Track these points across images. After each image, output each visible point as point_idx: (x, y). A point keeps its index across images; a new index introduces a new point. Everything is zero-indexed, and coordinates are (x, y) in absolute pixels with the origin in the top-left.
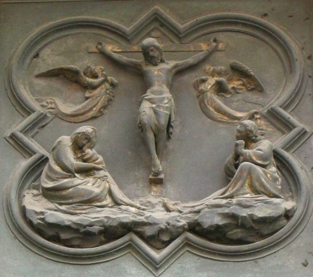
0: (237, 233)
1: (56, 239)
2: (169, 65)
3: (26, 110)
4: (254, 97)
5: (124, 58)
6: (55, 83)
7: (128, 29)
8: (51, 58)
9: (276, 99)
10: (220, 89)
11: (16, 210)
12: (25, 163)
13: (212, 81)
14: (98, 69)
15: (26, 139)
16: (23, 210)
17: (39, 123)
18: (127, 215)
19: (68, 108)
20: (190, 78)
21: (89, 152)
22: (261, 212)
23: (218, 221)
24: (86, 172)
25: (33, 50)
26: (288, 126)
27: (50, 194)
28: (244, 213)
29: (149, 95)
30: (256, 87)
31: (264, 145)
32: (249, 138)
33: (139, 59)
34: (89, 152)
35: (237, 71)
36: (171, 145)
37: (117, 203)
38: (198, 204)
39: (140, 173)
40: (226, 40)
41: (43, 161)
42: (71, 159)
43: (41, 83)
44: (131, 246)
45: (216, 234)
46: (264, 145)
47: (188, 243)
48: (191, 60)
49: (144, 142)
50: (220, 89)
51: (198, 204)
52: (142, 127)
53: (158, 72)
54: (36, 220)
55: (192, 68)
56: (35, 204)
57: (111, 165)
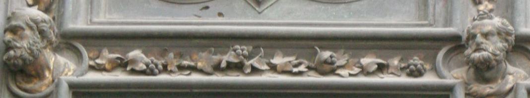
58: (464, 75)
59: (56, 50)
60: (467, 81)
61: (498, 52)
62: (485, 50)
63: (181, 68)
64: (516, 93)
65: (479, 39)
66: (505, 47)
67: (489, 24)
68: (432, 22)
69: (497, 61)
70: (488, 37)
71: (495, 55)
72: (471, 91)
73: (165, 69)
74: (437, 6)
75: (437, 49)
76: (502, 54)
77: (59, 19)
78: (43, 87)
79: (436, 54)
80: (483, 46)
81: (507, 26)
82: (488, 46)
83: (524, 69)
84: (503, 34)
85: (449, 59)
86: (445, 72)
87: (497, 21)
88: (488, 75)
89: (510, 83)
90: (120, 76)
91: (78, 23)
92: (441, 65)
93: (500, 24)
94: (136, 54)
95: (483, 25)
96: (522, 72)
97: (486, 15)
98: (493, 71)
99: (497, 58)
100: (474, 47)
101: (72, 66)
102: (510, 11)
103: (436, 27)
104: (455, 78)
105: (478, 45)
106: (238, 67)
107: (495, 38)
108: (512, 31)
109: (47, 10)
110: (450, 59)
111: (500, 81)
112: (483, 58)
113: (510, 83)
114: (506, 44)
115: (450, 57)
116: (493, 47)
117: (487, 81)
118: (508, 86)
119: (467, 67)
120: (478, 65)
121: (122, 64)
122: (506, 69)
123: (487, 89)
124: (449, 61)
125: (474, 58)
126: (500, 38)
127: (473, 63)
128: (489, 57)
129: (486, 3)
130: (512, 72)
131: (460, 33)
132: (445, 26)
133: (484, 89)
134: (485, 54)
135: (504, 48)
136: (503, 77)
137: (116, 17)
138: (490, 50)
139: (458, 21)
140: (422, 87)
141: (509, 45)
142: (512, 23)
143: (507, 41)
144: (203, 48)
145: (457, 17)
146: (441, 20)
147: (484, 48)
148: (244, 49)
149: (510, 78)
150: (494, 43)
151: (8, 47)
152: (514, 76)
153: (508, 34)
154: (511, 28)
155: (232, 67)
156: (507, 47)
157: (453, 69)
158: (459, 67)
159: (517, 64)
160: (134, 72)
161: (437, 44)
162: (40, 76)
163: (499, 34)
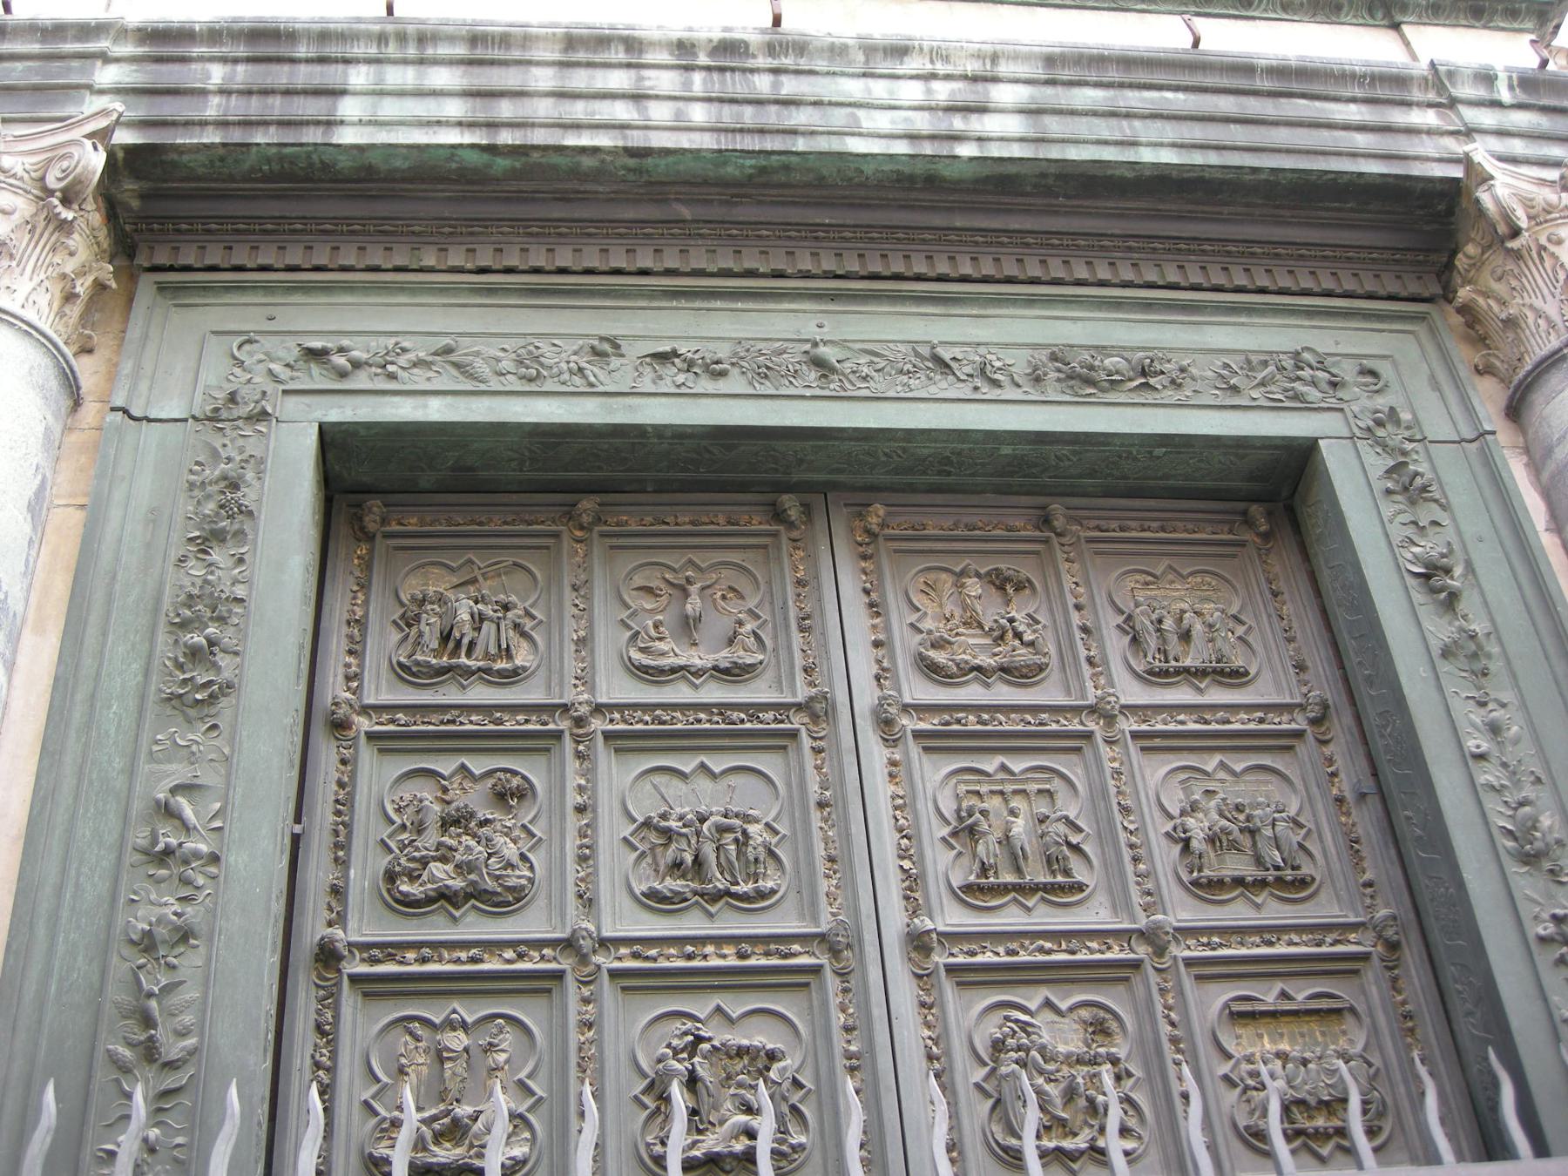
0: (737, 671)
1: (647, 673)
2: (699, 585)
3: (628, 607)
4: (740, 602)
5: (676, 582)
6: (641, 593)
7: (676, 566)
8: (638, 580)
9: (751, 603)
10: (724, 597)
11: (626, 658)
12: (629, 634)
13: (720, 594)
14: (662, 586)
15: (628, 622)
16: (630, 658)
17: (634, 614)
18: (681, 661)
19: (648, 607)
20: (709, 591)
21: (662, 629)
22: (749, 661)
23: (728, 665)
24: (660, 639)
25: (629, 577)
26: (759, 617)
27: (642, 650)
28: (740, 661)
29: (689, 600)
30: (742, 597)
31: (748, 627)
32: (741, 623)
33: (683, 582)
34: (662, 629)
35: (732, 589)
36: (701, 626)
37: (676, 655)
38: (717, 656)
39: (686, 640)
40: (725, 573)
41: (638, 633)
42: (653, 633)
43: (634, 593)
44: (683, 677)
45: (726, 671)
46: (748, 627)
47: (712, 676)
48: (708, 583)
49: (688, 624)
50: (724, 597)
51: (717, 656)
52: (687, 617)
53: (694, 589)
54: (636, 663)
55: (709, 587)
56: (636, 656)
57: (672, 637)
59: (359, 714)
63: (423, 723)
73: (415, 724)
77: (360, 698)
78: (352, 734)
87: (586, 696)
90: (391, 728)
91: (371, 701)
94: (400, 715)
101: (367, 722)
106: (453, 722)
109: (354, 694)
116: (584, 710)
121: (393, 721)
123: (581, 731)
137: (390, 697)
144: (434, 712)
148: (455, 712)
151: (333, 713)
155: (449, 722)
160: (399, 725)
162: (350, 728)
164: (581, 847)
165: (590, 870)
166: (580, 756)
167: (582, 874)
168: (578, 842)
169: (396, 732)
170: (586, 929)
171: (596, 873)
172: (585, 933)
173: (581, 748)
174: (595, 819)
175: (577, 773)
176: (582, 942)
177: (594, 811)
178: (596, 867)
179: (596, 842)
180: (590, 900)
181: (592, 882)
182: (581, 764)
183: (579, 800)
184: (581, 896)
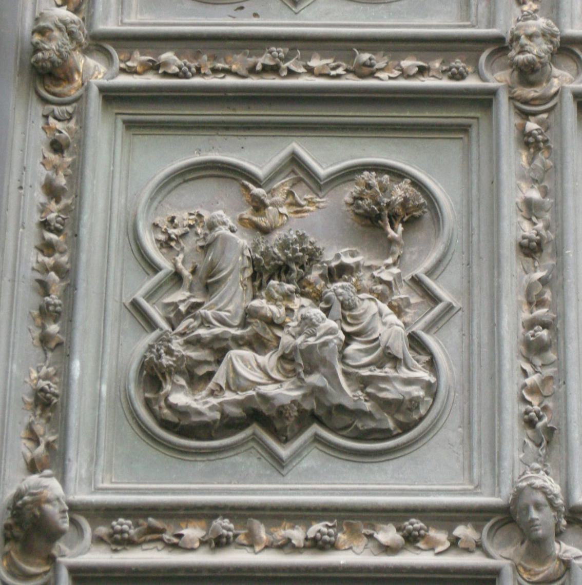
58: (508, 78)
59: (86, 52)
60: (510, 84)
61: (543, 54)
62: (529, 52)
63: (215, 71)
64: (561, 96)
65: (523, 40)
66: (550, 49)
67: (534, 25)
68: (474, 23)
69: (541, 63)
70: (532, 39)
71: (540, 57)
72: (515, 95)
73: (198, 72)
74: (479, 6)
75: (479, 51)
76: (547, 56)
77: (89, 20)
78: (72, 91)
79: (479, 56)
80: (527, 48)
81: (552, 27)
82: (532, 48)
83: (570, 71)
84: (548, 35)
85: (491, 62)
86: (488, 75)
87: (541, 22)
88: (532, 78)
89: (556, 87)
90: (152, 80)
91: (108, 24)
92: (483, 67)
93: (544, 25)
94: (168, 56)
95: (528, 26)
96: (567, 75)
97: (530, 16)
98: (538, 74)
99: (542, 60)
100: (518, 49)
101: (103, 69)
102: (555, 11)
103: (479, 28)
104: (499, 81)
105: (522, 46)
106: (273, 70)
107: (540, 40)
108: (557, 32)
109: (76, 11)
110: (493, 62)
111: (544, 84)
112: (528, 60)
113: (556, 87)
114: (551, 46)
115: (493, 59)
116: (537, 49)
117: (531, 84)
118: (553, 90)
119: (510, 70)
120: (523, 68)
121: (154, 67)
122: (551, 72)
124: (492, 64)
125: (518, 61)
126: (545, 39)
127: (517, 66)
128: (533, 58)
129: (531, 3)
130: (557, 75)
131: (504, 34)
132: (488, 27)
133: (529, 92)
134: (529, 56)
135: (549, 50)
136: (548, 81)
137: (148, 18)
138: (535, 52)
139: (502, 22)
140: (366, 249)
141: (554, 47)
142: (558, 24)
143: (552, 42)
144: (237, 50)
145: (501, 18)
146: (484, 20)
147: (529, 50)
148: (280, 51)
149: (556, 81)
150: (539, 45)
151: (36, 49)
152: (559, 80)
153: (553, 35)
154: (556, 29)
155: (268, 70)
156: (553, 49)
157: (497, 72)
158: (502, 70)
159: (563, 66)
160: (166, 75)
161: (480, 46)
162: (69, 79)
163: (544, 35)
164: (531, 324)
165: (548, 371)
166: (529, 142)
167: (533, 379)
168: (526, 315)
169: (160, 89)
170: (543, 490)
171: (561, 377)
172: (540, 497)
173: (531, 126)
174: (560, 268)
175: (523, 177)
176: (534, 514)
177: (558, 253)
178: (561, 366)
179: (562, 316)
180: (550, 431)
181: (553, 395)
182: (531, 160)
183: (528, 230)
184: (530, 423)
